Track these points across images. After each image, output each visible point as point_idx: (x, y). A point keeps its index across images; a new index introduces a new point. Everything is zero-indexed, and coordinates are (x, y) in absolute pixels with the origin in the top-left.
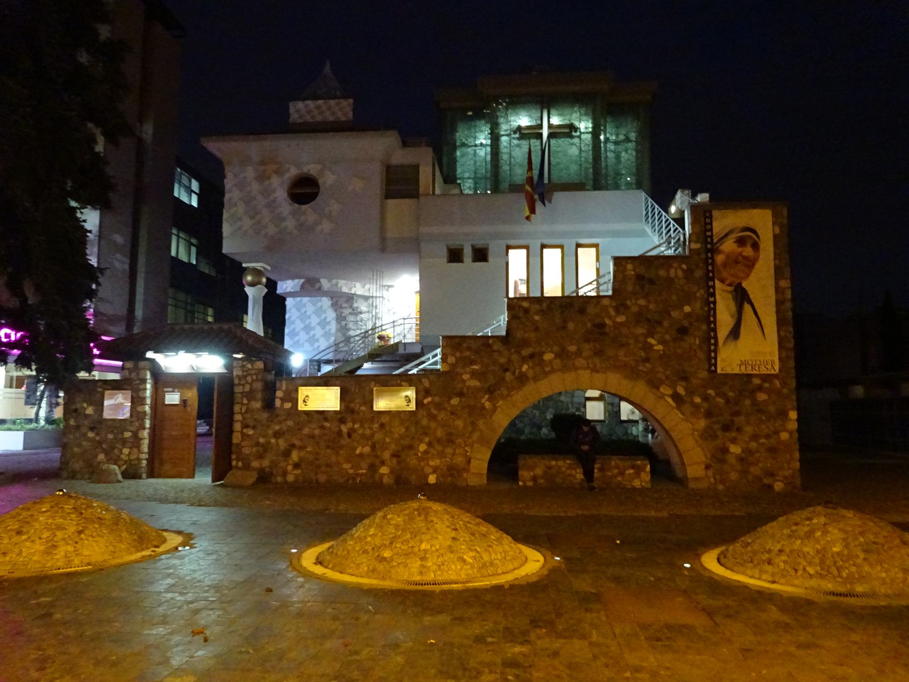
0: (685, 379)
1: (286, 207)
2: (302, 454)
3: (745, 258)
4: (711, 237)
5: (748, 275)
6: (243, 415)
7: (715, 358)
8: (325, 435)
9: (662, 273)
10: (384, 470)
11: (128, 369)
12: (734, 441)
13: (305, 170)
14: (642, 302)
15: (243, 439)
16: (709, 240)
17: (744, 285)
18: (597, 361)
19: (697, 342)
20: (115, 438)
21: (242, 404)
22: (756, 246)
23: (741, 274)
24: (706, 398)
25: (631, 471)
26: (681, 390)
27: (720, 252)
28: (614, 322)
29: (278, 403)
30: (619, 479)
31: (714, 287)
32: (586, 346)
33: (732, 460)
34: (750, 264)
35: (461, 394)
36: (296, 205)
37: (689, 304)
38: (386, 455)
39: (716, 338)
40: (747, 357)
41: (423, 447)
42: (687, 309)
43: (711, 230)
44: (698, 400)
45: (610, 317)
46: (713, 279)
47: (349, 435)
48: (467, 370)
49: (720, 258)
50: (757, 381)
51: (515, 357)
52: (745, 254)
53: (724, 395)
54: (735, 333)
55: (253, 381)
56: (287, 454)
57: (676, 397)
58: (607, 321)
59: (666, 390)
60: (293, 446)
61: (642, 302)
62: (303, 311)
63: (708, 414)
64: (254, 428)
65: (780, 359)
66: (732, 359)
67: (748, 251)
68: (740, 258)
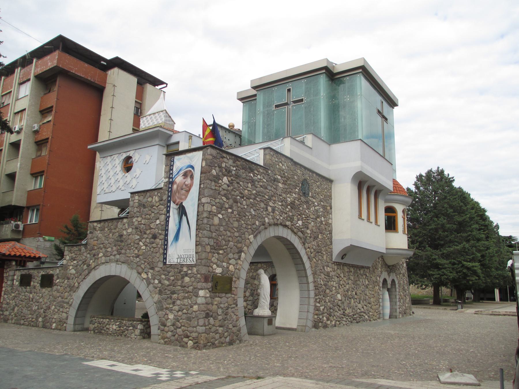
0: (152, 268)
3: (186, 185)
4: (172, 174)
7: (166, 254)
10: (40, 319)
12: (171, 311)
17: (183, 204)
18: (118, 257)
22: (192, 177)
23: (183, 197)
24: (160, 282)
25: (131, 328)
27: (176, 183)
28: (127, 233)
31: (170, 207)
32: (115, 248)
35: (68, 279)
37: (158, 219)
39: (167, 240)
40: (182, 253)
42: (158, 222)
43: (172, 170)
44: (156, 282)
46: (169, 201)
49: (175, 187)
51: (88, 255)
52: (186, 183)
53: (168, 280)
56: (13, 309)
57: (147, 279)
58: (125, 233)
59: (144, 276)
63: (160, 293)
64: (7, 295)
67: (188, 181)
68: (184, 186)
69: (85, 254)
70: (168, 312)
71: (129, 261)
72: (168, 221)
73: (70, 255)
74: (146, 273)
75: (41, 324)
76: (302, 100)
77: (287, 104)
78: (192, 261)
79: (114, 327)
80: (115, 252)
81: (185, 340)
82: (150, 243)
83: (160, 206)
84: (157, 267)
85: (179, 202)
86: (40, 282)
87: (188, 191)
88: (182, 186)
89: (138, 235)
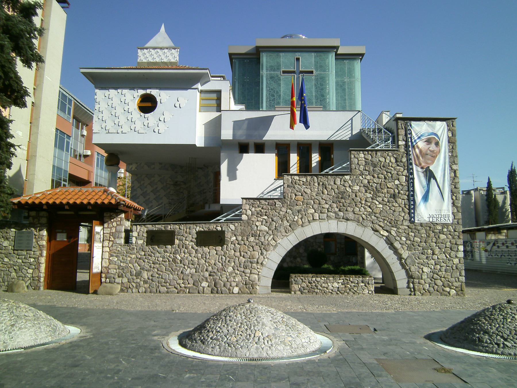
1: (137, 114)
2: (150, 273)
3: (430, 151)
4: (411, 138)
5: (433, 162)
6: (109, 248)
7: (414, 213)
8: (165, 262)
9: (382, 160)
11: (33, 217)
13: (148, 91)
14: (368, 177)
15: (110, 264)
16: (410, 140)
17: (431, 168)
18: (341, 214)
19: (403, 203)
20: (23, 262)
21: (109, 240)
22: (437, 144)
23: (429, 162)
25: (362, 284)
26: (393, 233)
29: (134, 240)
30: (356, 289)
31: (412, 169)
32: (335, 205)
33: (425, 277)
34: (434, 156)
36: (142, 114)
38: (207, 274)
39: (414, 200)
41: (230, 269)
42: (397, 182)
43: (411, 134)
44: (404, 239)
45: (350, 186)
47: (181, 261)
48: (259, 219)
50: (439, 228)
54: (426, 198)
55: (117, 225)
56: (138, 275)
60: (142, 269)
61: (368, 177)
62: (142, 182)
63: (409, 248)
65: (453, 213)
66: (425, 212)
67: (433, 147)
68: (429, 152)
69: (284, 209)
70: (422, 266)
71: (361, 219)
72: (413, 183)
73: (253, 209)
74: (387, 231)
75: (208, 290)
76: (312, 72)
77: (294, 72)
78: (450, 220)
79: (336, 285)
80: (337, 210)
81: (448, 289)
82: (388, 202)
83: (398, 167)
84: (402, 225)
85: (424, 166)
86: (194, 240)
87: (434, 157)
88: (426, 151)
89: (370, 193)
